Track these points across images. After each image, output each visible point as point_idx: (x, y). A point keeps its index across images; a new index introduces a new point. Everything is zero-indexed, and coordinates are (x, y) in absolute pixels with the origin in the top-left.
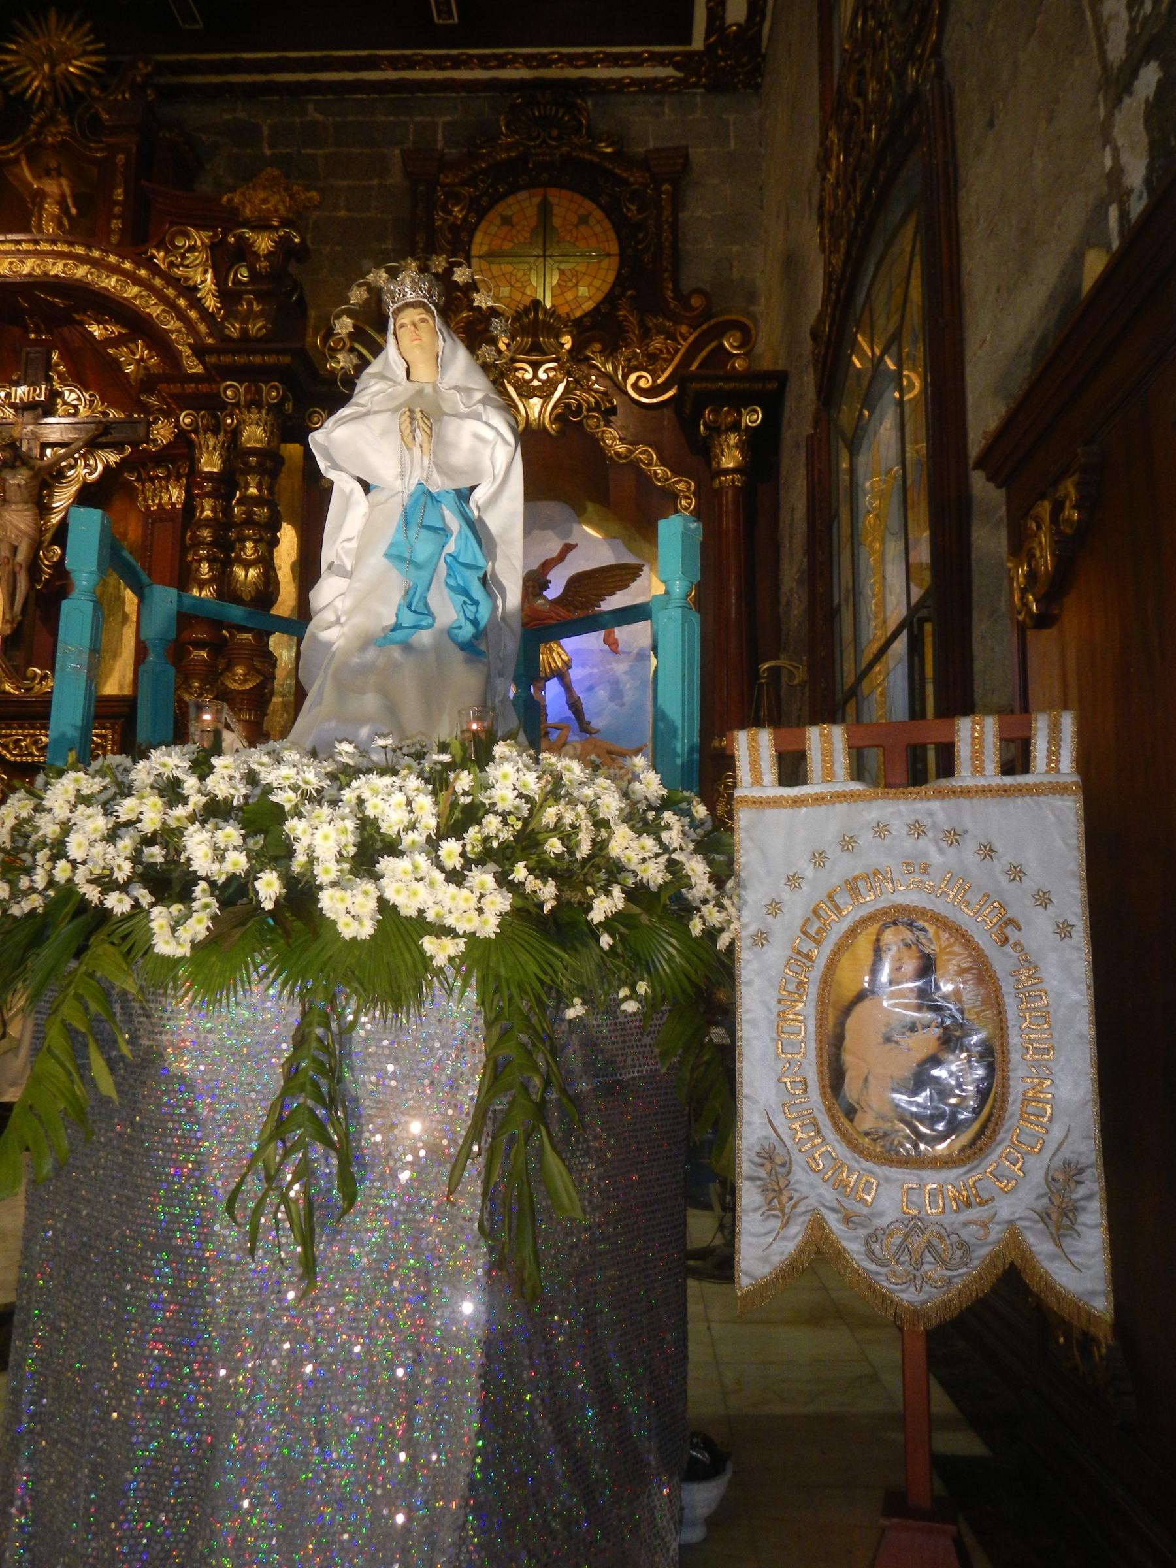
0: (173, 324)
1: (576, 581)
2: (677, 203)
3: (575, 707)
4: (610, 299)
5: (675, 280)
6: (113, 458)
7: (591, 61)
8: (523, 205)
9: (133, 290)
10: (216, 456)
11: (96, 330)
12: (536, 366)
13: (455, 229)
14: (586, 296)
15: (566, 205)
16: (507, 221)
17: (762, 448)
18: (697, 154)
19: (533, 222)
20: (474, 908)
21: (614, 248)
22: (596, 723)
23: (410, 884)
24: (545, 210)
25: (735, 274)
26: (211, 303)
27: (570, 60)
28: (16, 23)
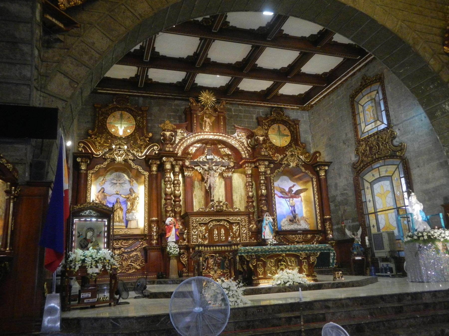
0: (240, 148)
1: (297, 191)
5: (300, 140)
7: (288, 106)
8: (275, 126)
10: (251, 171)
11: (220, 146)
12: (292, 157)
15: (282, 127)
16: (273, 129)
19: (277, 129)
21: (290, 134)
24: (279, 127)
25: (307, 140)
26: (246, 145)
27: (284, 105)
28: (201, 92)
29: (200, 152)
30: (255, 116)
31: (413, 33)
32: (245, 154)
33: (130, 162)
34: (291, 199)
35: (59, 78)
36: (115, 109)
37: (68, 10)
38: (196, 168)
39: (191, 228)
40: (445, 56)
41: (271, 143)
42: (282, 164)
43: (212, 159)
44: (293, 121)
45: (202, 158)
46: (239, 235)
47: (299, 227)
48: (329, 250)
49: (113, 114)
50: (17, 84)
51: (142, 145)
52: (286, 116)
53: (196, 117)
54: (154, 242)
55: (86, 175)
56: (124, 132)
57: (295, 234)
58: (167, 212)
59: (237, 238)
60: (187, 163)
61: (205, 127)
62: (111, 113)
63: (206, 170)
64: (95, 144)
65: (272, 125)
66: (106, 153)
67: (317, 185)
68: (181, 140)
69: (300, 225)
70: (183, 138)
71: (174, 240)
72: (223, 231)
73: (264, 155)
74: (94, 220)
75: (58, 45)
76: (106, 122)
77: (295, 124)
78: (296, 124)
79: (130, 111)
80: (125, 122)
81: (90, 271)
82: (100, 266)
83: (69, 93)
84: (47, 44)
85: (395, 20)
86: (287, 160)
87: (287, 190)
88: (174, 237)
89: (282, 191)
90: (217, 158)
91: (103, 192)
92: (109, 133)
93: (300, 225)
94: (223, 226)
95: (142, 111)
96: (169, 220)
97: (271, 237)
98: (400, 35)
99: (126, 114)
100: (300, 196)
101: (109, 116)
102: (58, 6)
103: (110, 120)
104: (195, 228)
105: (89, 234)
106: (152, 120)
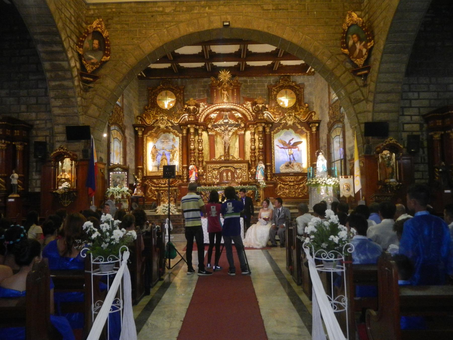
2: (303, 91)
3: (294, 158)
4: (295, 104)
6: (237, 128)
8: (283, 91)
9: (241, 109)
11: (233, 112)
13: (275, 95)
14: (292, 104)
15: (289, 91)
17: (318, 128)
18: (306, 84)
20: (333, 183)
21: (295, 97)
22: (296, 159)
23: (331, 183)
26: (251, 111)
29: (220, 117)
30: (266, 84)
31: (316, 42)
32: (250, 117)
33: (170, 128)
34: (290, 149)
35: (93, 107)
36: (161, 90)
37: (94, 72)
38: (216, 129)
39: (208, 171)
40: (342, 56)
42: (281, 123)
43: (228, 122)
44: (298, 86)
45: (221, 122)
46: (241, 177)
47: (293, 171)
48: (255, 189)
49: (161, 93)
50: (72, 116)
51: (180, 114)
52: (293, 82)
53: (216, 92)
54: (185, 180)
55: (142, 138)
56: (169, 105)
57: (288, 176)
58: (191, 161)
59: (239, 178)
60: (210, 126)
61: (224, 98)
62: (160, 92)
63: (223, 131)
64: (149, 115)
65: (280, 91)
66: (154, 123)
67: (310, 138)
68: (203, 110)
69: (294, 169)
70: (205, 109)
71: (194, 180)
72: (229, 174)
73: (261, 119)
74: (120, 173)
75: (91, 89)
76: (156, 100)
77: (301, 88)
78: (301, 88)
79: (172, 90)
80: (170, 99)
81: (115, 197)
82: (121, 195)
83: (97, 114)
84: (86, 90)
85: (301, 34)
86: (285, 120)
87: (287, 142)
88: (194, 177)
89: (284, 143)
90: (232, 121)
91: (155, 148)
92: (158, 107)
93: (294, 169)
94: (230, 171)
96: (191, 167)
97: (263, 178)
98: (303, 46)
99: (170, 93)
100: (297, 147)
101: (158, 94)
102: (87, 72)
103: (159, 97)
104: (209, 172)
105: (118, 180)
106: (187, 95)
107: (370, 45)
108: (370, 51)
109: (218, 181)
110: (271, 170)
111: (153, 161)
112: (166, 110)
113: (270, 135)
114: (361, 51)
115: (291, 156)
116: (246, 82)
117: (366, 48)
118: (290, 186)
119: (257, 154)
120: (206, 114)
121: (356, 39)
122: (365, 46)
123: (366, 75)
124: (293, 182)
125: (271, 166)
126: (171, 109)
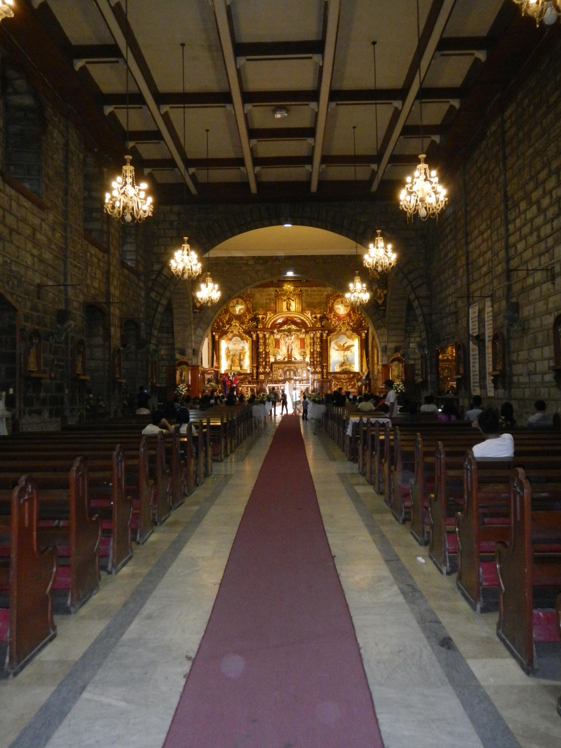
17: (367, 334)
41: (335, 312)
55: (219, 341)
65: (336, 299)
68: (270, 318)
87: (342, 344)
94: (292, 370)
95: (250, 298)
99: (240, 301)
107: (385, 292)
108: (385, 295)
109: (283, 378)
110: (327, 370)
111: (227, 360)
112: (237, 316)
113: (327, 340)
114: (380, 295)
115: (345, 357)
116: (307, 291)
117: (383, 293)
118: (343, 383)
119: (315, 355)
120: (272, 321)
121: (377, 286)
122: (382, 292)
123: (384, 310)
124: (346, 379)
125: (327, 366)
126: (242, 315)
